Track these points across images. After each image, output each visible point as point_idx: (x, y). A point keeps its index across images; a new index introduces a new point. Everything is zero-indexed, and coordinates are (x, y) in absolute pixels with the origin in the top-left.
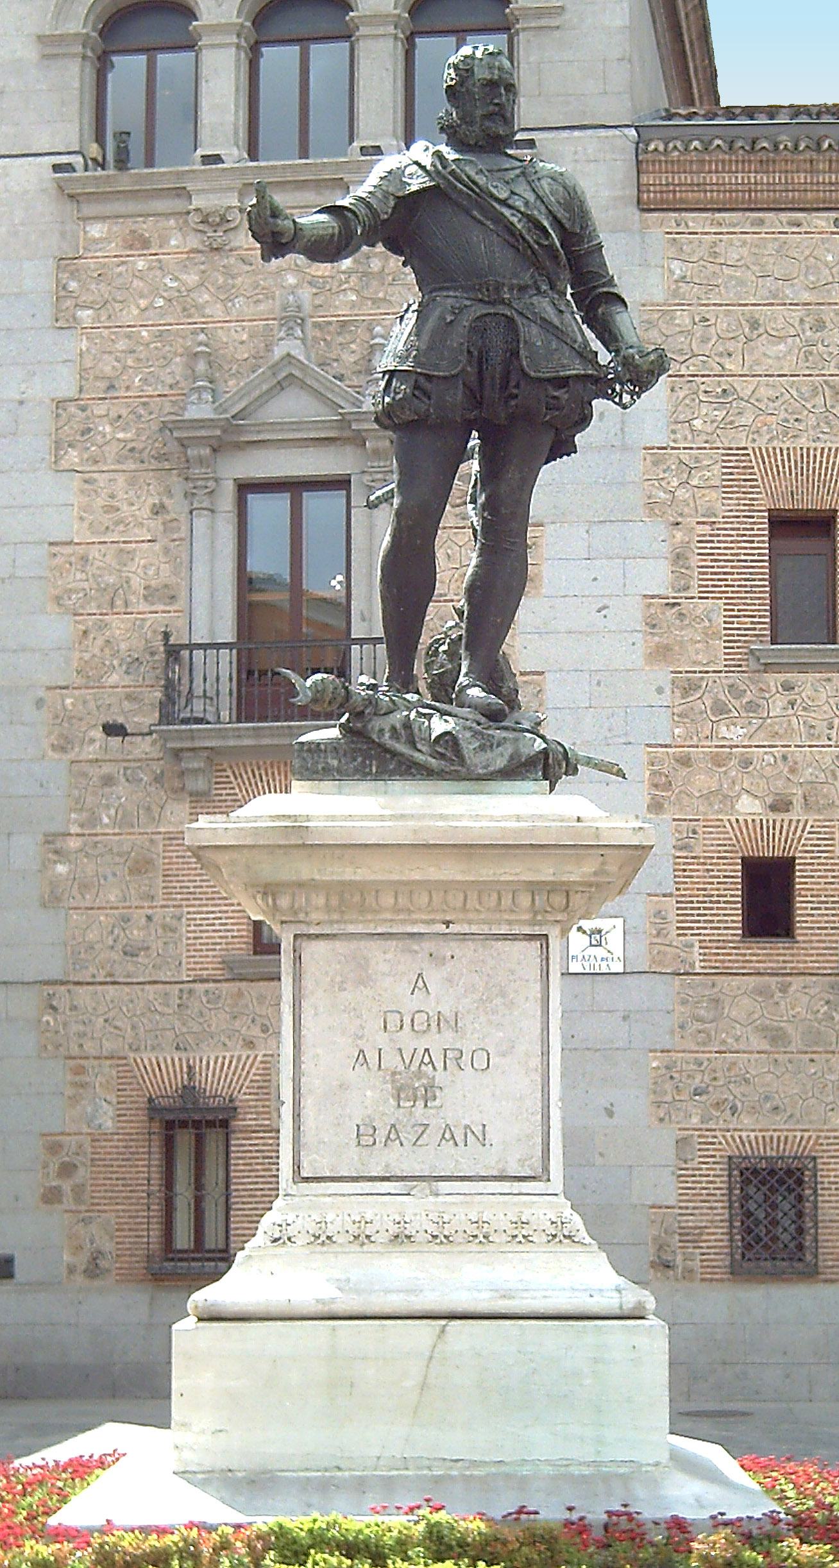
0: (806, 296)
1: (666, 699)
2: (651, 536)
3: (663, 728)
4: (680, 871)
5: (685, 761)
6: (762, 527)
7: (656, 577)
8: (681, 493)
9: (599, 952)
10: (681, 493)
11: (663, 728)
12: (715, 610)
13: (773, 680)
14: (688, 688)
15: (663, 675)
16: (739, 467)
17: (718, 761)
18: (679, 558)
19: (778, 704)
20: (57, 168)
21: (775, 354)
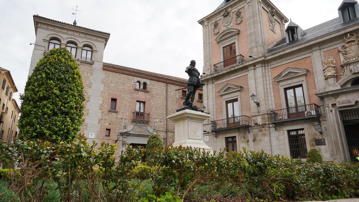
0: (116, 80)
1: (101, 113)
2: (101, 99)
3: (100, 116)
4: (100, 129)
5: (102, 119)
6: (111, 100)
7: (101, 102)
8: (104, 95)
9: (92, 136)
10: (104, 95)
11: (100, 116)
12: (106, 106)
13: (110, 113)
14: (103, 113)
15: (101, 111)
16: (109, 94)
17: (105, 120)
18: (103, 101)
19: (110, 115)
20: (44, 52)
21: (113, 85)
